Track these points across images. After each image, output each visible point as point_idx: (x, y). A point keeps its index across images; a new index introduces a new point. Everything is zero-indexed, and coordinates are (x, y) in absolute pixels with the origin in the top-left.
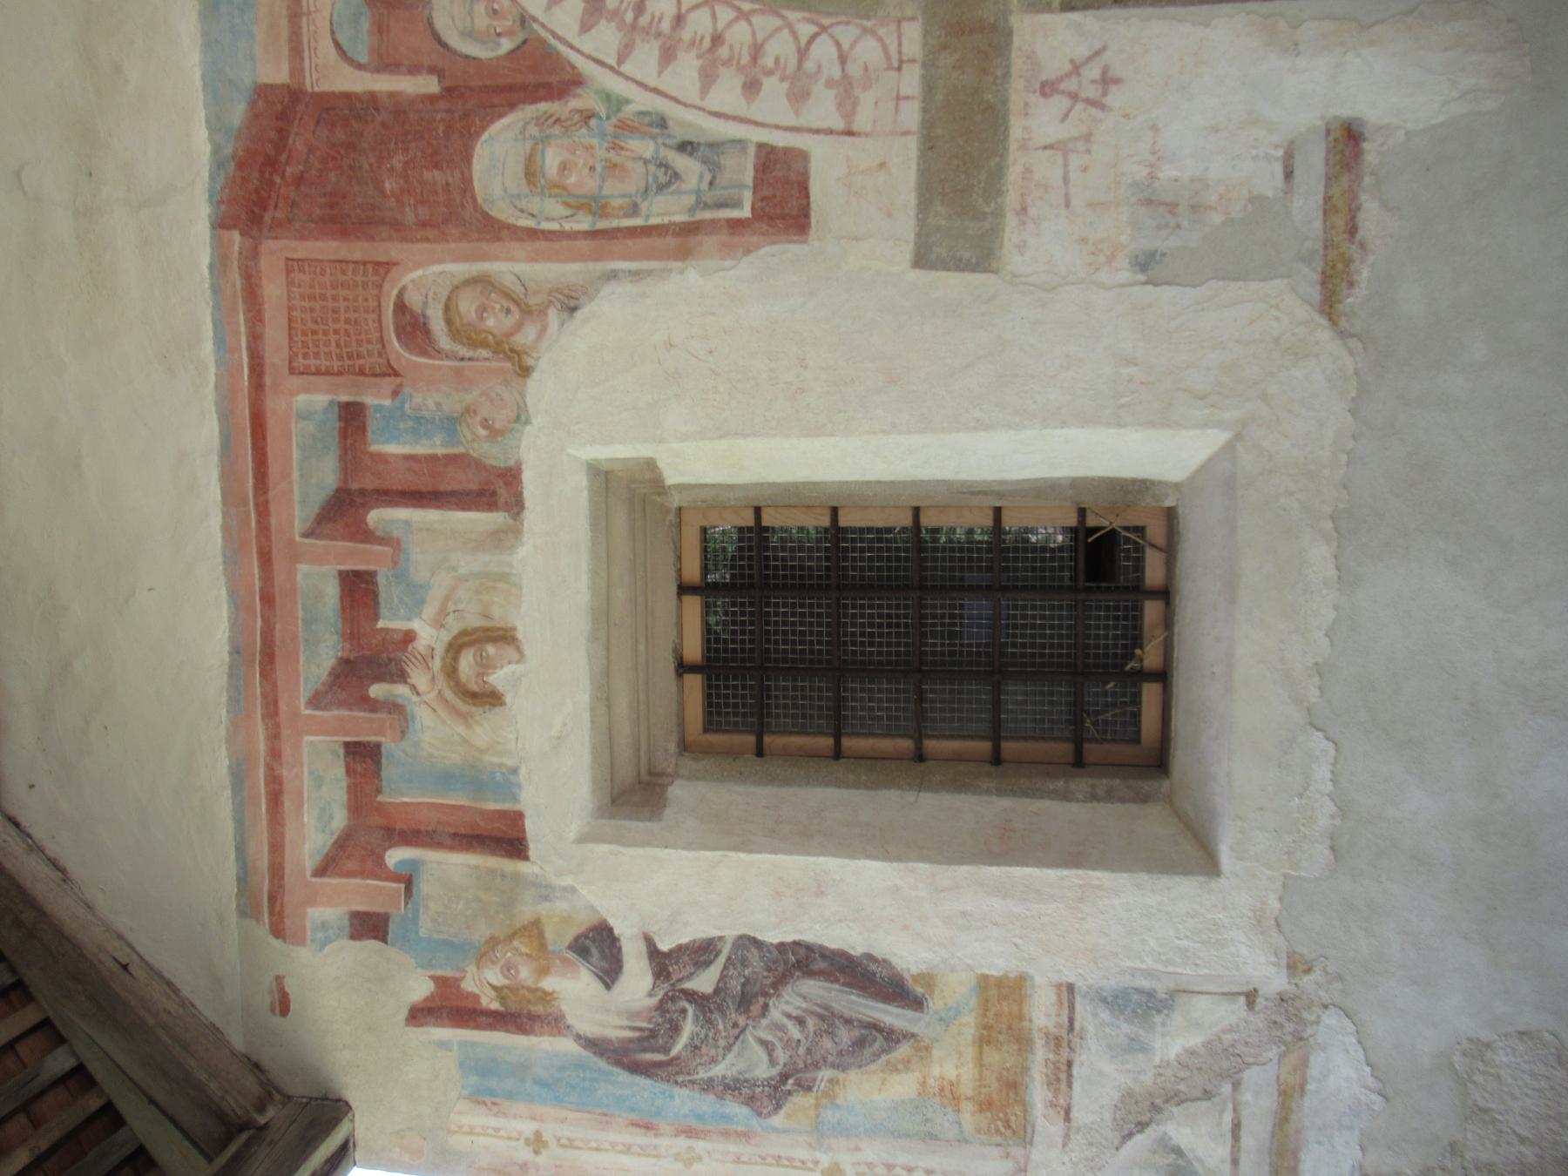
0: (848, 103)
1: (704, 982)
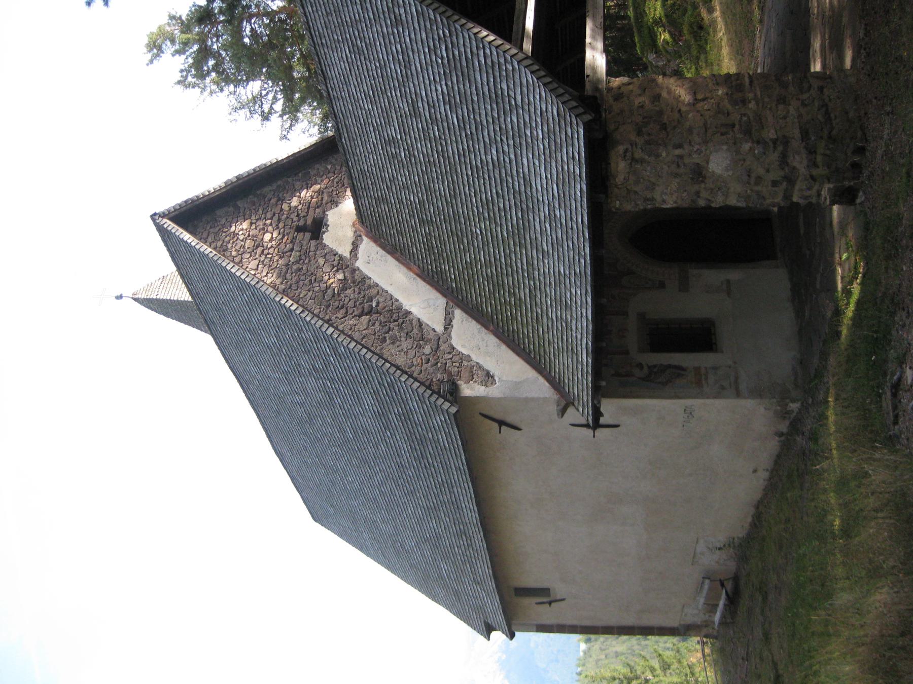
1: (655, 370)
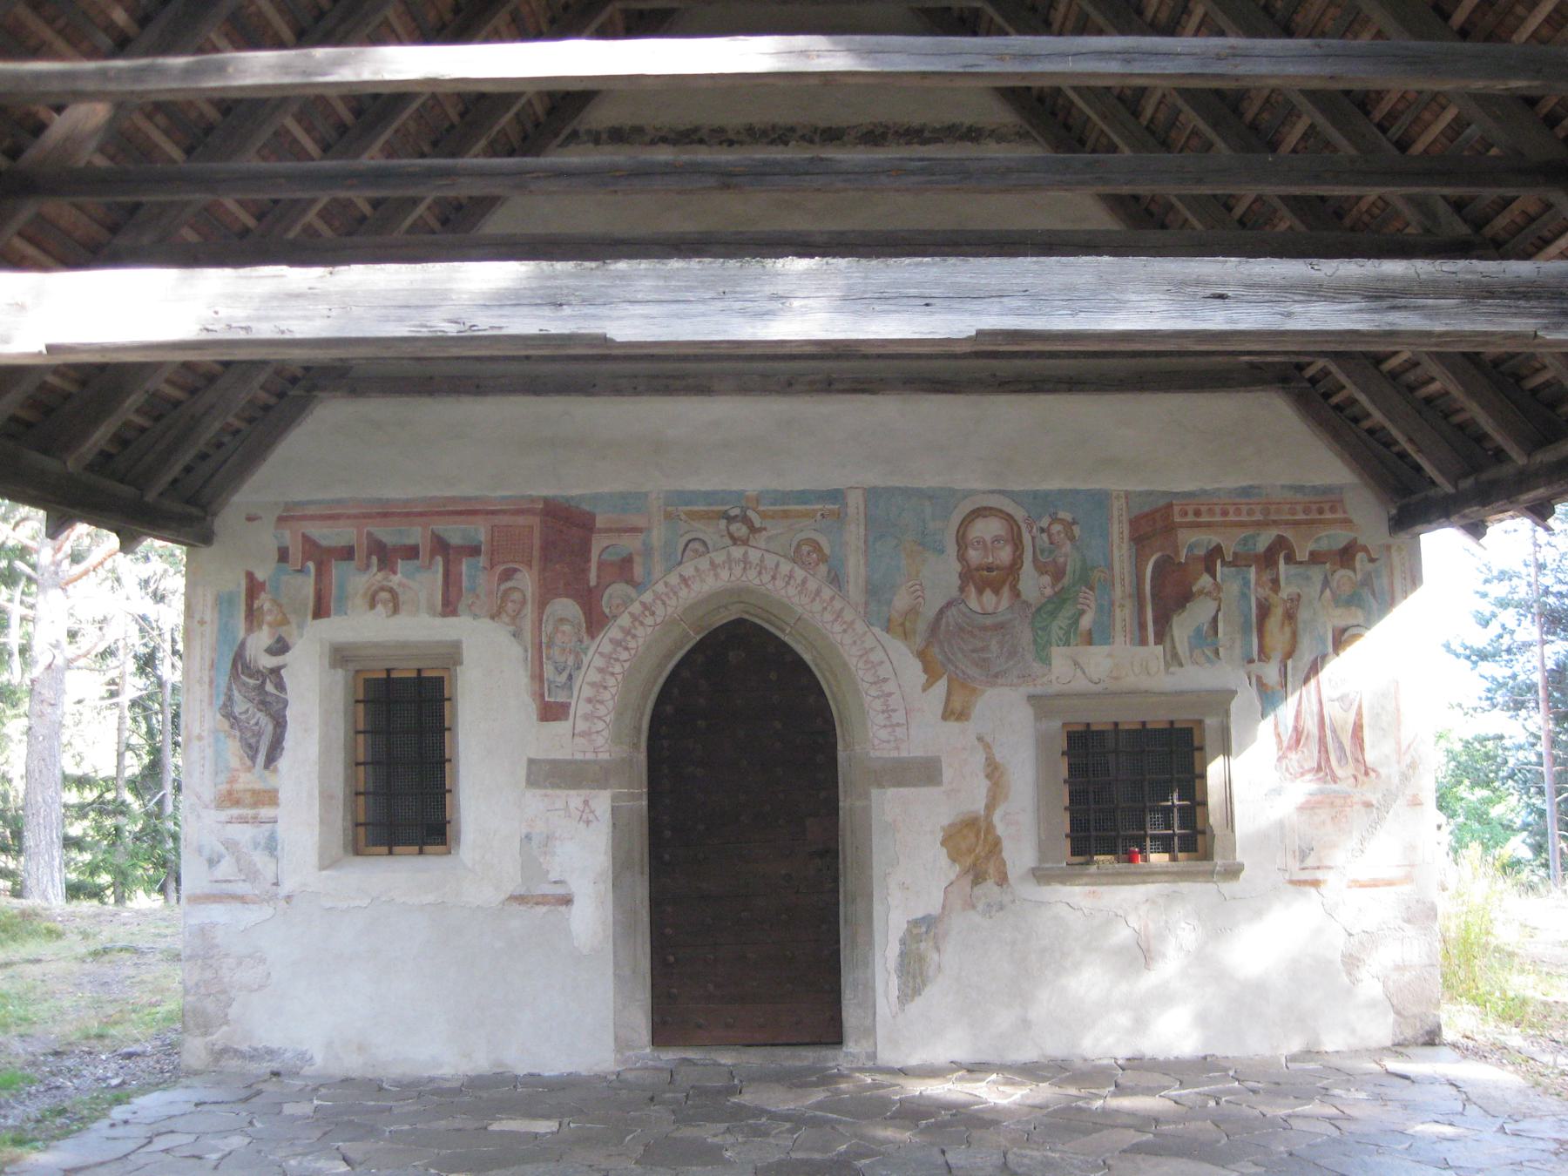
0: (583, 734)
1: (269, 687)
